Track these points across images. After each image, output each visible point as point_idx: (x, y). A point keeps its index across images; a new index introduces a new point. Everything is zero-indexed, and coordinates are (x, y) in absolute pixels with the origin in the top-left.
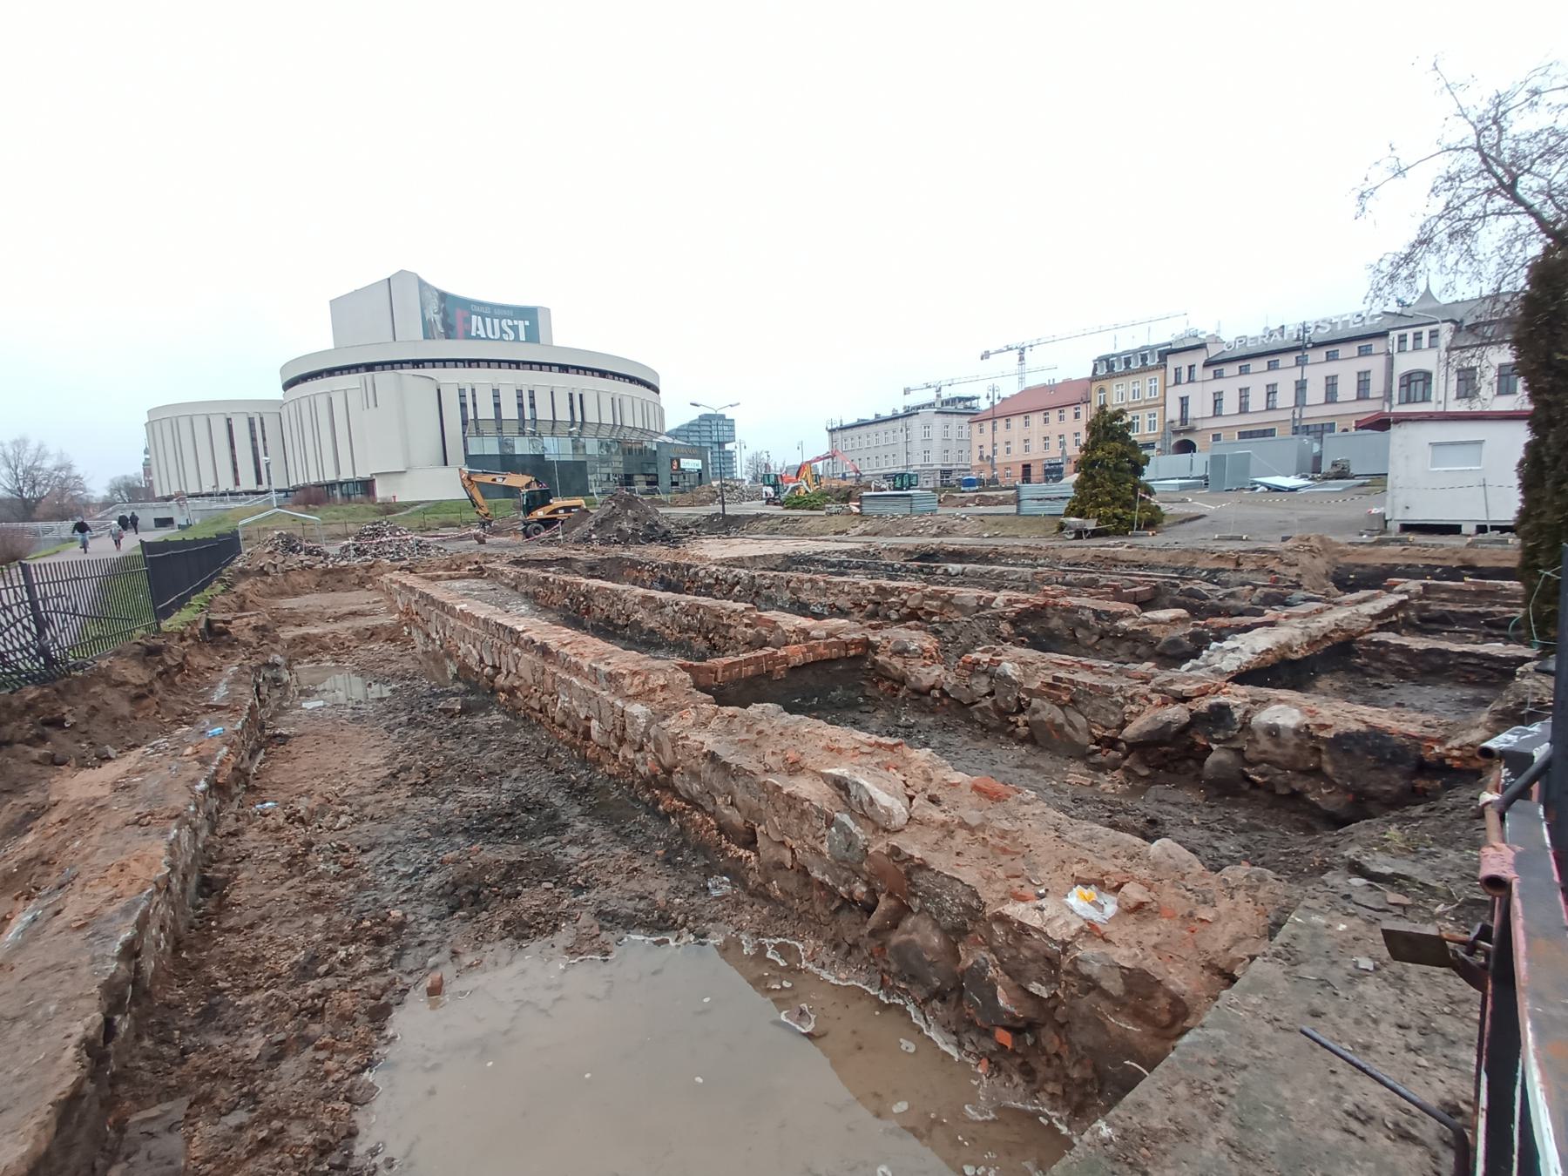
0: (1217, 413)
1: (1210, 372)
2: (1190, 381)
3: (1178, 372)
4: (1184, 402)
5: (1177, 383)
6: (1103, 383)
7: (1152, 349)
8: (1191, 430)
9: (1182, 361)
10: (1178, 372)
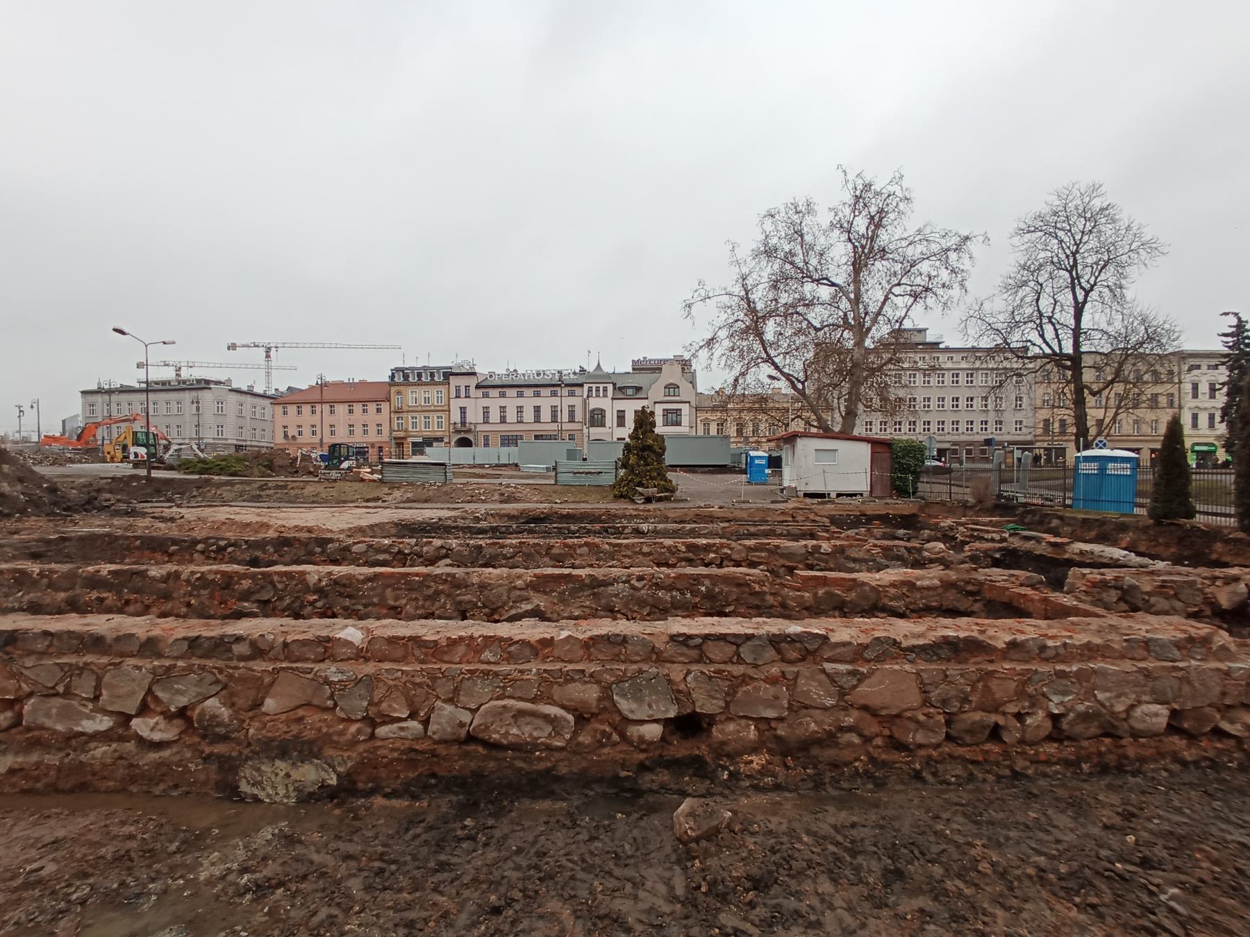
0: (486, 421)
1: (480, 393)
2: (467, 397)
4: (463, 410)
5: (458, 397)
7: (438, 369)
8: (469, 431)
9: (462, 382)
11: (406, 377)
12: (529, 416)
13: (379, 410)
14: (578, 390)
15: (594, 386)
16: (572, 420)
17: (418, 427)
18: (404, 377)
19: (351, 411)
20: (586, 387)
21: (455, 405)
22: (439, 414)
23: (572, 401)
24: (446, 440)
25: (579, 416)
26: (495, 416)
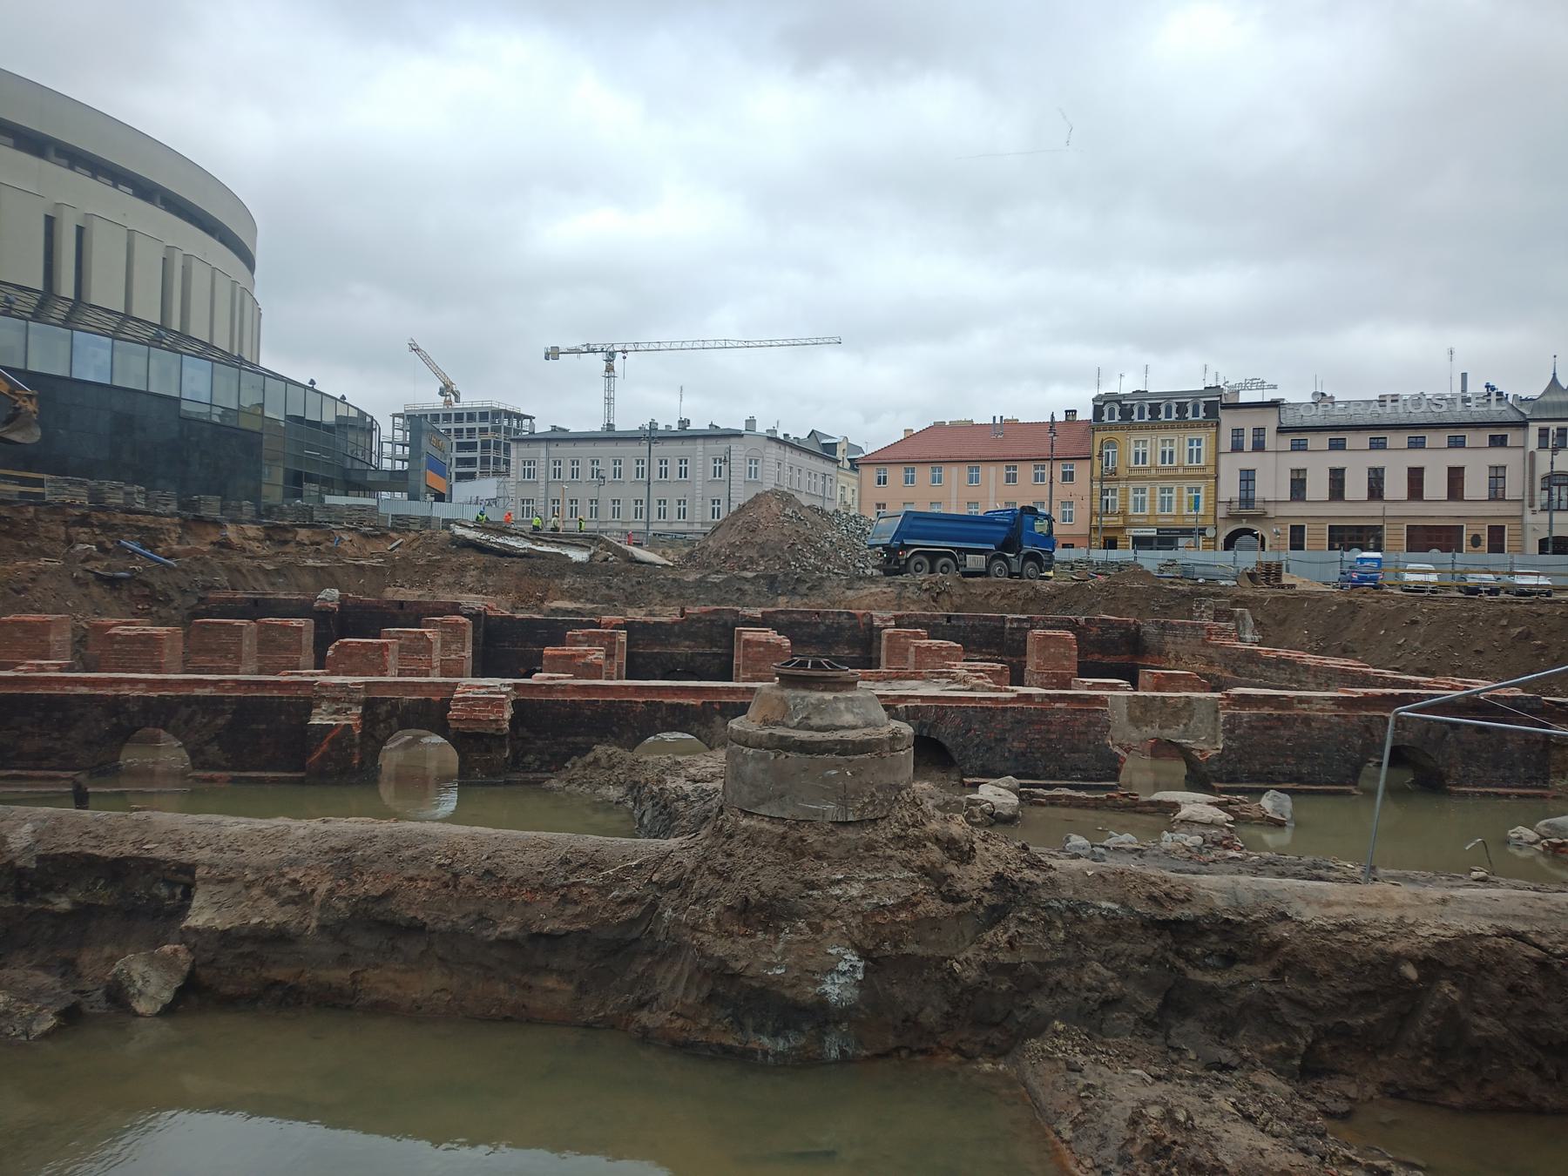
2: (1259, 447)
4: (1247, 477)
5: (1237, 448)
8: (1261, 517)
9: (1248, 422)
10: (1238, 433)
11: (1126, 413)
12: (1396, 486)
13: (1068, 477)
17: (1149, 506)
18: (1119, 413)
19: (1011, 478)
21: (1231, 467)
22: (1194, 484)
24: (1210, 533)
26: (1318, 487)
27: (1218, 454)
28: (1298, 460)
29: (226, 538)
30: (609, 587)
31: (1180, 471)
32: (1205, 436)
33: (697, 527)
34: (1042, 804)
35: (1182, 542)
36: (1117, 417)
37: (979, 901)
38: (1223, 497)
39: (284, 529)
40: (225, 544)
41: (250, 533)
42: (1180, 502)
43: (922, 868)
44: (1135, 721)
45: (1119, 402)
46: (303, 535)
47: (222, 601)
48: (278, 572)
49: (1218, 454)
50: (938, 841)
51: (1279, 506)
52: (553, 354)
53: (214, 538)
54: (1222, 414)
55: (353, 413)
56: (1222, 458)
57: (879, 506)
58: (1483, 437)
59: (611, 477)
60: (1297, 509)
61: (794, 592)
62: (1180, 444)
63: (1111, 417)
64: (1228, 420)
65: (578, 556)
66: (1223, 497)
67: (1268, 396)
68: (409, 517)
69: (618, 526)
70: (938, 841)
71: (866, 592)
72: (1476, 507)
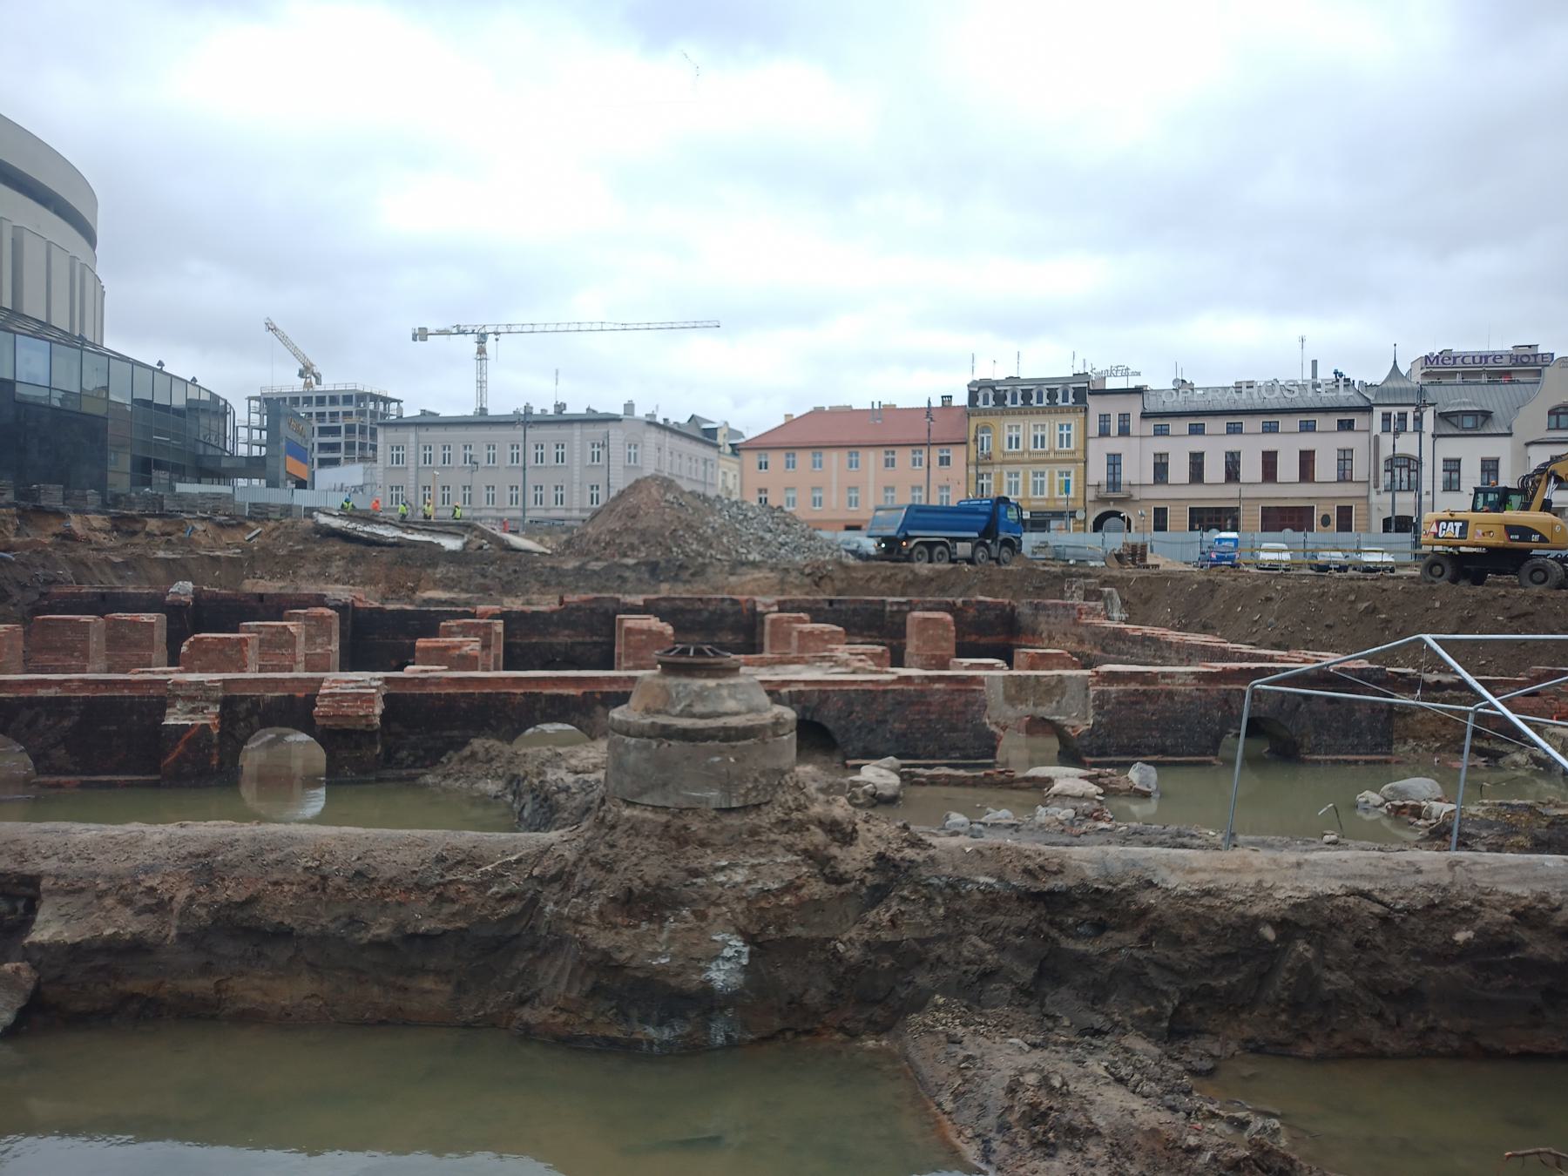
2: (1124, 432)
3: (1104, 418)
4: (1114, 461)
5: (1104, 433)
6: (989, 420)
9: (1114, 407)
10: (1104, 418)
11: (1000, 398)
12: (1251, 469)
13: (945, 461)
14: (1359, 421)
15: (1395, 411)
16: (1344, 477)
18: (994, 398)
19: (890, 463)
20: (1378, 413)
22: (1064, 467)
23: (1346, 440)
24: (1080, 516)
25: (1360, 469)
26: (1179, 470)
27: (1086, 438)
28: (1161, 444)
29: (70, 529)
30: (484, 576)
31: (1052, 456)
32: (1074, 421)
33: (576, 514)
34: (922, 784)
35: (1054, 524)
36: (991, 402)
37: (862, 881)
38: (1092, 480)
39: (133, 519)
40: (68, 537)
41: (96, 524)
42: (1051, 485)
43: (805, 851)
44: (1011, 700)
45: (993, 388)
46: (153, 525)
47: (60, 595)
48: (127, 564)
49: (1086, 438)
50: (821, 823)
51: (1144, 489)
52: (421, 335)
53: (58, 529)
54: (1090, 400)
55: (205, 397)
56: (1091, 442)
57: (760, 491)
58: (1331, 421)
59: (484, 463)
60: (1160, 492)
61: (676, 579)
62: (1051, 429)
63: (986, 402)
64: (1096, 406)
65: (451, 544)
66: (1092, 480)
67: (1133, 383)
68: (268, 505)
69: (493, 513)
70: (821, 823)
71: (749, 577)
72: (1325, 491)
